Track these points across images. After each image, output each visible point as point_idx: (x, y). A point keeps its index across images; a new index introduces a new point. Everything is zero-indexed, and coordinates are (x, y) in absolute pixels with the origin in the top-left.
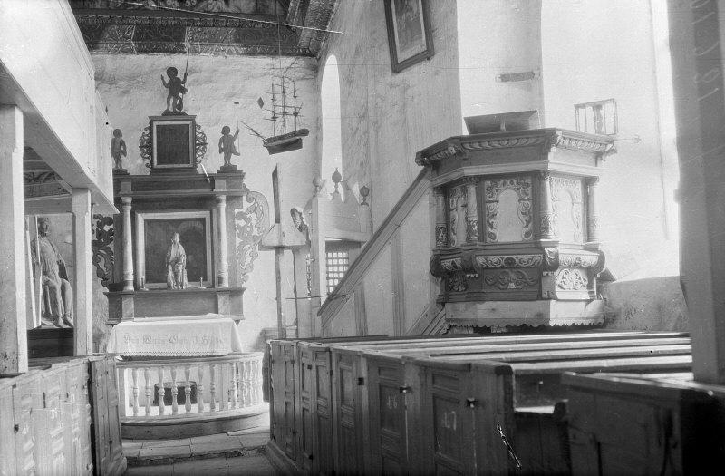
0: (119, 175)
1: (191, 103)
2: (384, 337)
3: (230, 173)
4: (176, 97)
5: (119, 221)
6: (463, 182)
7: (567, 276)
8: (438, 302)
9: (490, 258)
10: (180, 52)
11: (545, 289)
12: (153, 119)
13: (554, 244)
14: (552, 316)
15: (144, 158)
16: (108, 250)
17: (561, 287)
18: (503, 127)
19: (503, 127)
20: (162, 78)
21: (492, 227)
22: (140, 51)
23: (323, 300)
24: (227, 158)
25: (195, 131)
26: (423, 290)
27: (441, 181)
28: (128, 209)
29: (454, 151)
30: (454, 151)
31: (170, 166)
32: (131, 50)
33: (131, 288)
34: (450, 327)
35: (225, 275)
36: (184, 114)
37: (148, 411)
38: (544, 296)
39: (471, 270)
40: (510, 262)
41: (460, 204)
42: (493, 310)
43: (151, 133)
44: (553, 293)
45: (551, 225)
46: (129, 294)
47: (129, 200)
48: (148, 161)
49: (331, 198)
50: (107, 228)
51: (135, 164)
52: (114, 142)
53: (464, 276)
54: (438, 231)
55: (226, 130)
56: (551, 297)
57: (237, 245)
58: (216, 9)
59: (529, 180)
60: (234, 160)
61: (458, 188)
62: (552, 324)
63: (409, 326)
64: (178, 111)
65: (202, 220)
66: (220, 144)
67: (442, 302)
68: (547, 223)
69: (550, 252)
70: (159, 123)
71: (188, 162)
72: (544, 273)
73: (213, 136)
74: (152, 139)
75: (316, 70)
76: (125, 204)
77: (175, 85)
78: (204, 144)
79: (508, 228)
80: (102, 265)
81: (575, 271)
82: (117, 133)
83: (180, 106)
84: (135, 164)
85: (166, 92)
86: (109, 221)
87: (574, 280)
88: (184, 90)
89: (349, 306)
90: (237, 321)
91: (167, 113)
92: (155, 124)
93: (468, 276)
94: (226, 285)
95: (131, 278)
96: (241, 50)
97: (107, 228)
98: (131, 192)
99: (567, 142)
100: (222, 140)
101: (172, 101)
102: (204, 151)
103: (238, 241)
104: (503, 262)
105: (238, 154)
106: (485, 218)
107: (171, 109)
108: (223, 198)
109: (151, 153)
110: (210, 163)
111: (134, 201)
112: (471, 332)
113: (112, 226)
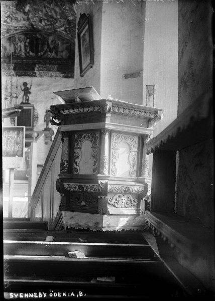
1: (31, 97)
4: (27, 96)
10: (35, 76)
14: (104, 224)
17: (115, 206)
24: (47, 125)
25: (34, 112)
42: (72, 217)
44: (106, 209)
56: (105, 212)
58: (51, 57)
62: (104, 230)
64: (27, 102)
77: (27, 91)
78: (38, 118)
83: (28, 100)
88: (30, 93)
96: (62, 75)
99: (127, 111)
101: (24, 98)
102: (37, 121)
109: (14, 122)
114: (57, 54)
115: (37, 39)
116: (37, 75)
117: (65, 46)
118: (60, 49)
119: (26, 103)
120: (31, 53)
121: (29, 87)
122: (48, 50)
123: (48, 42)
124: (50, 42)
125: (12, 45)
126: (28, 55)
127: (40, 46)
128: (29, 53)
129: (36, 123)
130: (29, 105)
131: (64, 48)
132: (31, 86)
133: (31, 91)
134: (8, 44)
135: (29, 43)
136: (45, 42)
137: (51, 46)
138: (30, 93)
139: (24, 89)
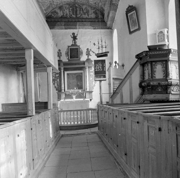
0: (60, 61)
2: (127, 104)
3: (88, 60)
4: (75, 41)
5: (60, 74)
6: (147, 63)
7: (174, 88)
8: (141, 94)
9: (154, 83)
10: (76, 29)
11: (169, 91)
12: (69, 47)
13: (171, 79)
15: (66, 57)
16: (57, 81)
18: (157, 48)
19: (157, 48)
20: (71, 36)
21: (155, 75)
22: (65, 29)
23: (112, 94)
24: (88, 57)
26: (137, 91)
27: (142, 63)
28: (62, 71)
29: (145, 55)
30: (145, 55)
31: (73, 59)
32: (63, 29)
33: (63, 91)
34: (144, 101)
35: (88, 88)
36: (77, 45)
37: (67, 123)
38: (168, 93)
39: (149, 86)
40: (159, 84)
41: (147, 68)
43: (68, 50)
44: (171, 92)
45: (170, 74)
46: (63, 93)
47: (63, 68)
48: (68, 58)
49: (114, 67)
50: (57, 75)
51: (65, 59)
52: (58, 53)
53: (147, 88)
54: (141, 75)
55: (88, 49)
57: (91, 79)
59: (164, 62)
60: (90, 57)
61: (146, 65)
62: (170, 100)
63: (134, 100)
64: (75, 44)
65: (82, 73)
66: (86, 53)
67: (142, 94)
68: (169, 74)
69: (170, 81)
70: (71, 48)
71: (78, 58)
72: (168, 87)
73: (85, 51)
74: (68, 52)
75: (112, 33)
76: (62, 69)
77: (75, 38)
78: (82, 53)
79: (159, 74)
80: (56, 85)
81: (177, 86)
82: (59, 50)
84: (65, 59)
85: (72, 39)
86: (57, 74)
87: (176, 88)
88: (77, 39)
89: (119, 96)
90: (91, 100)
91: (72, 45)
92: (69, 48)
93: (148, 87)
94: (88, 90)
95: (63, 88)
96: (92, 28)
97: (57, 75)
98: (63, 66)
100: (87, 52)
103: (91, 78)
104: (157, 84)
105: (91, 56)
106: (153, 72)
107: (73, 44)
108: (87, 67)
109: (68, 56)
110: (84, 58)
112: (149, 102)
113: (58, 75)
114: (88, 15)
115: (76, 7)
116: (77, 28)
117: (93, 11)
118: (90, 13)
119: (74, 45)
120: (73, 16)
121: (76, 36)
122: (83, 13)
123: (83, 9)
124: (84, 9)
125: (62, 11)
126: (71, 16)
127: (78, 11)
128: (71, 15)
129: (82, 56)
130: (76, 46)
131: (93, 12)
133: (77, 38)
134: (59, 10)
135: (72, 10)
136: (81, 9)
137: (85, 11)
138: (77, 39)
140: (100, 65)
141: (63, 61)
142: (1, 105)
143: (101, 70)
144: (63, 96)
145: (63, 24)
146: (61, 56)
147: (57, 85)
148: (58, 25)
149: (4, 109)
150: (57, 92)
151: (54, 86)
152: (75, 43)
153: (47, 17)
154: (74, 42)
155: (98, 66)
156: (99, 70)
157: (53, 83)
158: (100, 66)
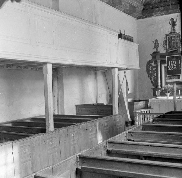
5: (157, 67)
12: (167, 35)
16: (154, 76)
20: (169, 22)
22: (165, 14)
28: (159, 64)
32: (163, 15)
33: (160, 87)
46: (159, 89)
47: (159, 61)
50: (154, 69)
52: (155, 44)
82: (156, 41)
84: (162, 50)
85: (171, 26)
86: (154, 67)
88: (176, 25)
91: (171, 33)
95: (160, 84)
97: (154, 69)
98: (159, 59)
107: (172, 31)
111: (161, 62)
113: (155, 69)
132: (176, 20)
138: (176, 25)
139: (172, 22)
140: (174, 62)
141: (161, 52)
142: (75, 107)
143: (175, 68)
144: (157, 93)
145: (162, 9)
146: (159, 47)
147: (154, 79)
148: (157, 12)
149: (78, 109)
150: (154, 87)
151: (151, 81)
152: (174, 30)
153: (145, 3)
154: (173, 29)
155: (171, 63)
156: (172, 68)
157: (150, 77)
158: (174, 64)
